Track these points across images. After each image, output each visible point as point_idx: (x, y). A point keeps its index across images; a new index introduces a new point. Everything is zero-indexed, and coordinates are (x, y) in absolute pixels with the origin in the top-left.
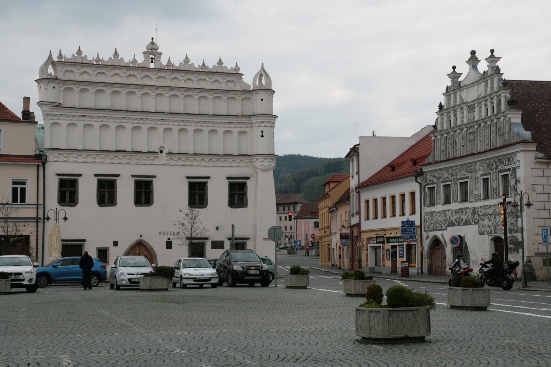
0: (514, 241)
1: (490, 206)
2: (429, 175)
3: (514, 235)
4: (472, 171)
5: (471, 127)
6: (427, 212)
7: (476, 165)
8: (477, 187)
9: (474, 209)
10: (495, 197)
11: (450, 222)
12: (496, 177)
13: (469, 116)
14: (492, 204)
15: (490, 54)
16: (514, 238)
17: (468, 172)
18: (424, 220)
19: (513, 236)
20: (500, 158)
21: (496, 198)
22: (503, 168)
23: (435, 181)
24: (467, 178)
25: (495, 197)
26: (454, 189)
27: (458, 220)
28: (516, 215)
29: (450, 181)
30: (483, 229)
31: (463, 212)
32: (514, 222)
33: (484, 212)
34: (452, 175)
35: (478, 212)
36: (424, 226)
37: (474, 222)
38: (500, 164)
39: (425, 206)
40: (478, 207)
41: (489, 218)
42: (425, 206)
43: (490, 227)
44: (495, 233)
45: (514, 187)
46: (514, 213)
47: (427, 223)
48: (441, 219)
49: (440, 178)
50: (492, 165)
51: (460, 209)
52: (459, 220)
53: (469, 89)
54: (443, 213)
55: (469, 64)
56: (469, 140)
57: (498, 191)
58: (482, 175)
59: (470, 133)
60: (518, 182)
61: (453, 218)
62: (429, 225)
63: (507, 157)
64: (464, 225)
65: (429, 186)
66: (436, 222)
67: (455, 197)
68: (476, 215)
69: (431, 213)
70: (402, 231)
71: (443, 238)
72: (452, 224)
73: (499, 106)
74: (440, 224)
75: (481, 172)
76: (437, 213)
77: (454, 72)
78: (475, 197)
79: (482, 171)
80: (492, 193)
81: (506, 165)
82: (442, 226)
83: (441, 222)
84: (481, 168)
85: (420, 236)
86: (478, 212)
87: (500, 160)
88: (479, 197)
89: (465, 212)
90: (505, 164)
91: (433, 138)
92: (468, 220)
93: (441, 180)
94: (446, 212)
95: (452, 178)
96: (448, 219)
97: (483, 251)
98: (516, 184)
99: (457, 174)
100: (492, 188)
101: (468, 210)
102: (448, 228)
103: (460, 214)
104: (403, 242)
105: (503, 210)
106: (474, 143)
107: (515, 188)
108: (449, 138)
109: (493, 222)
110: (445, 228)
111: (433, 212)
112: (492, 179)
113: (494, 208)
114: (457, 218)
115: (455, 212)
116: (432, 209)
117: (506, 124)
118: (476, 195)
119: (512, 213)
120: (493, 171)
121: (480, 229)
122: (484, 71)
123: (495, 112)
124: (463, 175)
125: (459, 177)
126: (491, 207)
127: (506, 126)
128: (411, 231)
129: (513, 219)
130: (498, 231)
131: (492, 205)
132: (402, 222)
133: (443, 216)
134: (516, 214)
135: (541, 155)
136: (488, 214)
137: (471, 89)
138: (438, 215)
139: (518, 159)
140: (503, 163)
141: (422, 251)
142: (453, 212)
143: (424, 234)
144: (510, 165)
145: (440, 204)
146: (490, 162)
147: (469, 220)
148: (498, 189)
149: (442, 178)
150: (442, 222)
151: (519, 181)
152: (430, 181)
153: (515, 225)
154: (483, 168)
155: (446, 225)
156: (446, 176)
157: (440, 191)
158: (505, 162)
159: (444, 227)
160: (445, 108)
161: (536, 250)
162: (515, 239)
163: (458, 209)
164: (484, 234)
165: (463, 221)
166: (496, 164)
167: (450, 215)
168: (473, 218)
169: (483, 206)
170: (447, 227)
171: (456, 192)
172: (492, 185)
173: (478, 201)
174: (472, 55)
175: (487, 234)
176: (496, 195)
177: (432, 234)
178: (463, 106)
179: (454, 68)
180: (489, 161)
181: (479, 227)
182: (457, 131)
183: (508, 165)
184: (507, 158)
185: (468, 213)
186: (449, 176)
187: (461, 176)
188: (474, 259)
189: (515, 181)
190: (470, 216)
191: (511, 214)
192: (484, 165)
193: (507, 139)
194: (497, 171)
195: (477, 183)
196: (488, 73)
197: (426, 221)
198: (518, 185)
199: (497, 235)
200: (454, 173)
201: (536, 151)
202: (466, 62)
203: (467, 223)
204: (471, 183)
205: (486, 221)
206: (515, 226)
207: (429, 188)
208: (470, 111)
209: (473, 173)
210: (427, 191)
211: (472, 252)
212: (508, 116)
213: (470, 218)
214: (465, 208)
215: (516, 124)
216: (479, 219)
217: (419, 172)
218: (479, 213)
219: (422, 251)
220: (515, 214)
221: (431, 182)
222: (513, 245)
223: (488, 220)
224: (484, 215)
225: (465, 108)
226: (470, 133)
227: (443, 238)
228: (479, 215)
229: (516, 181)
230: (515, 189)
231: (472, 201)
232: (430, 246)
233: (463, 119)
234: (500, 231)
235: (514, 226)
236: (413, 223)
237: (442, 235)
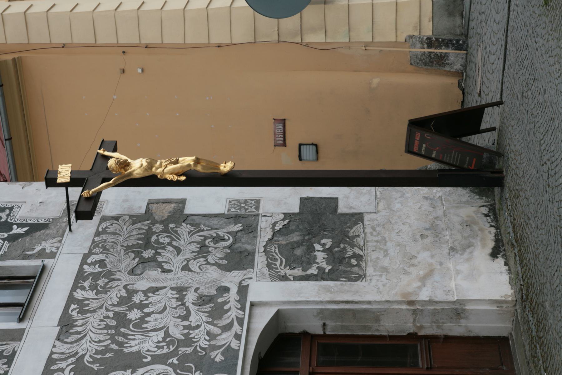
0: (295, 237)
16: (283, 240)
28: (165, 222)
32: (196, 238)
107: (22, 231)
119: (147, 245)
129: (181, 244)
130: (226, 338)
134: (161, 222)
162: (285, 231)
191: (147, 254)
206: (221, 233)
220: (158, 227)
222: (317, 247)
234: (227, 328)
235: (217, 239)
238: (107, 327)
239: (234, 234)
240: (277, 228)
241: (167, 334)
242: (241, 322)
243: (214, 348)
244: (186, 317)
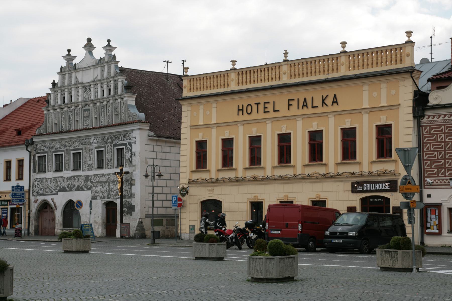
0: (127, 205)
1: (104, 175)
2: (40, 145)
3: (128, 200)
4: (86, 144)
5: (86, 105)
6: (36, 178)
7: (91, 138)
8: (91, 158)
9: (87, 177)
10: (109, 167)
11: (61, 187)
12: (111, 150)
13: (84, 95)
14: (106, 173)
15: (107, 43)
16: (127, 203)
17: (82, 144)
18: (33, 186)
19: (127, 201)
20: (116, 134)
21: (111, 168)
22: (119, 143)
23: (46, 150)
24: (81, 149)
25: (109, 167)
26: (67, 159)
27: (70, 186)
28: (131, 183)
29: (63, 151)
30: (96, 195)
31: (76, 179)
32: (128, 189)
33: (97, 179)
34: (65, 146)
35: (91, 179)
36: (33, 191)
37: (87, 188)
38: (116, 139)
39: (34, 172)
40: (91, 175)
41: (102, 185)
42: (34, 172)
43: (103, 193)
44: (108, 198)
45: (129, 159)
46: (128, 181)
47: (36, 188)
48: (52, 185)
49: (52, 148)
50: (108, 139)
51: (72, 176)
52: (71, 186)
53: (84, 71)
54: (54, 180)
55: (85, 49)
56: (84, 116)
57: (112, 162)
58: (96, 148)
59: (85, 110)
60: (133, 155)
61: (65, 185)
62: (39, 190)
63: (123, 133)
64: (76, 190)
65: (39, 155)
66: (46, 187)
67: (67, 166)
68: (89, 182)
69: (41, 180)
70: (12, 195)
71: (53, 202)
72: (63, 190)
73: (115, 89)
74: (50, 189)
75: (95, 144)
76: (47, 179)
77: (69, 55)
78: (88, 166)
79: (97, 144)
80: (107, 163)
81: (121, 140)
82: (52, 191)
83: (52, 188)
84: (96, 141)
85: (28, 200)
86: (91, 179)
87: (116, 135)
88: (92, 166)
89: (77, 179)
90: (120, 140)
91: (45, 112)
92: (80, 186)
93: (53, 150)
94: (58, 179)
95: (65, 149)
96: (60, 185)
97: (95, 214)
98: (131, 157)
99: (71, 146)
100: (106, 159)
101: (80, 178)
102: (59, 193)
103: (72, 181)
104: (7, 205)
105: (120, 179)
106: (89, 119)
107: (130, 160)
108: (62, 113)
109: (107, 188)
110: (56, 193)
111: (43, 178)
112: (106, 152)
113: (108, 177)
114: (69, 184)
115: (67, 179)
116: (42, 176)
117: (123, 105)
118: (89, 164)
119: (126, 181)
120: (109, 144)
121: (92, 194)
122: (101, 58)
123: (112, 93)
124: (76, 146)
125: (72, 148)
126: (105, 176)
127: (122, 107)
128: (21, 195)
129: (127, 187)
130: (112, 197)
131: (106, 174)
132: (13, 187)
133: (53, 183)
134: (131, 182)
135: (152, 134)
136: (102, 182)
137: (87, 71)
138: (49, 181)
139: (134, 136)
140: (119, 138)
141: (29, 214)
142: (65, 179)
143: (33, 198)
144: (126, 140)
145: (50, 171)
146: (105, 137)
147: (82, 186)
148: (112, 160)
149: (54, 148)
150: (53, 188)
151: (134, 154)
152: (40, 150)
153: (129, 191)
154: (98, 142)
155: (57, 191)
156: (58, 147)
157: (51, 160)
158: (120, 137)
159: (54, 192)
160: (59, 85)
161: (147, 213)
162: (129, 203)
163: (70, 176)
164: (96, 199)
165: (75, 187)
166: (111, 139)
167: (62, 182)
168: (85, 185)
169: (96, 174)
170: (57, 192)
171: (69, 162)
172: (106, 157)
173: (91, 170)
174: (88, 41)
175: (100, 199)
176: (111, 166)
177: (41, 198)
178: (79, 85)
179: (69, 51)
180: (104, 136)
181: (92, 193)
182: (71, 107)
183: (124, 140)
184: (123, 134)
185: (80, 180)
186: (62, 147)
187: (74, 147)
188: (85, 221)
189: (130, 155)
190: (83, 182)
192: (99, 139)
193: (123, 118)
194: (112, 145)
195: (91, 154)
196: (104, 59)
197: (35, 187)
198: (133, 158)
199: (110, 200)
200: (67, 144)
201: (149, 130)
202: (83, 47)
203: (79, 189)
204: (85, 154)
205: (99, 188)
206: (129, 193)
207: (39, 156)
208: (86, 91)
209: (87, 145)
210: (37, 159)
211: (83, 215)
212: (125, 99)
213: (82, 184)
214: (77, 176)
215: (131, 106)
216: (92, 186)
217: (30, 141)
218: (91, 180)
219: (29, 214)
220: (129, 182)
221: (42, 151)
222: (126, 209)
223: (101, 187)
224: (97, 182)
225: (80, 87)
226: (85, 110)
227: (53, 202)
228: (92, 182)
229: (132, 154)
230: (130, 161)
231: (85, 170)
232: (38, 209)
233: (78, 98)
234: (113, 197)
235: (127, 192)
236: (23, 188)
237: (52, 200)
238: (114, 180)
239: (128, 195)
240: (129, 202)
241: (112, 189)
242: (114, 199)
243: (110, 196)
244: (115, 191)
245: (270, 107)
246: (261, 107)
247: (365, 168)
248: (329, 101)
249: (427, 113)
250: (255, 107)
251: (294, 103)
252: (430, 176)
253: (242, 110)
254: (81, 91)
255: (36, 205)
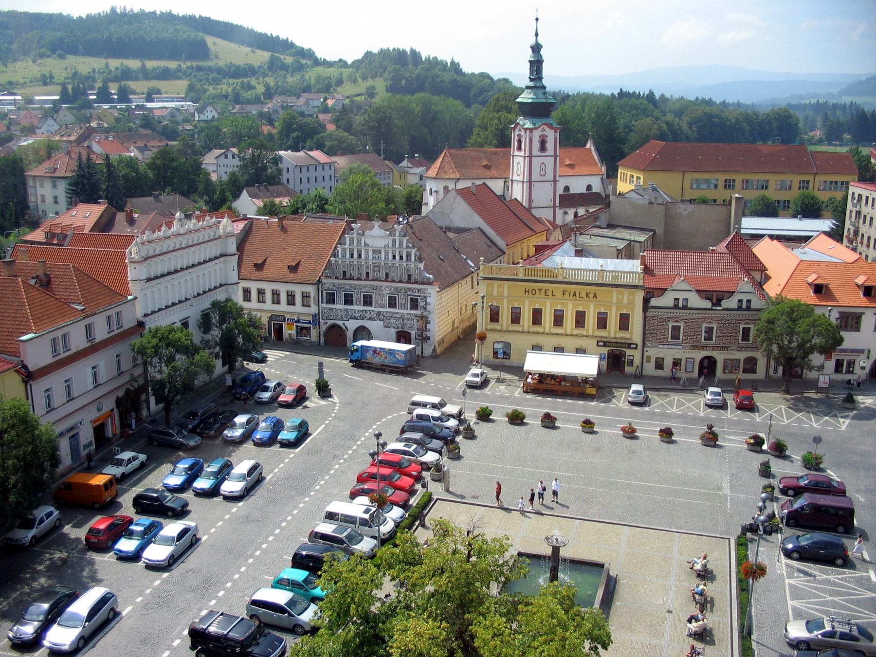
23: (334, 288)
33: (390, 315)
48: (344, 313)
61: (357, 315)
72: (355, 318)
95: (356, 291)
111: (333, 309)
177: (330, 322)
198: (428, 307)
203: (370, 319)
205: (392, 321)
224: (391, 317)
228: (384, 316)
237: (344, 324)
245: (549, 293)
246: (543, 292)
247: (612, 335)
248: (591, 295)
249: (650, 310)
250: (538, 292)
251: (567, 294)
252: (648, 341)
253: (529, 292)
254: (371, 253)
255: (326, 326)
